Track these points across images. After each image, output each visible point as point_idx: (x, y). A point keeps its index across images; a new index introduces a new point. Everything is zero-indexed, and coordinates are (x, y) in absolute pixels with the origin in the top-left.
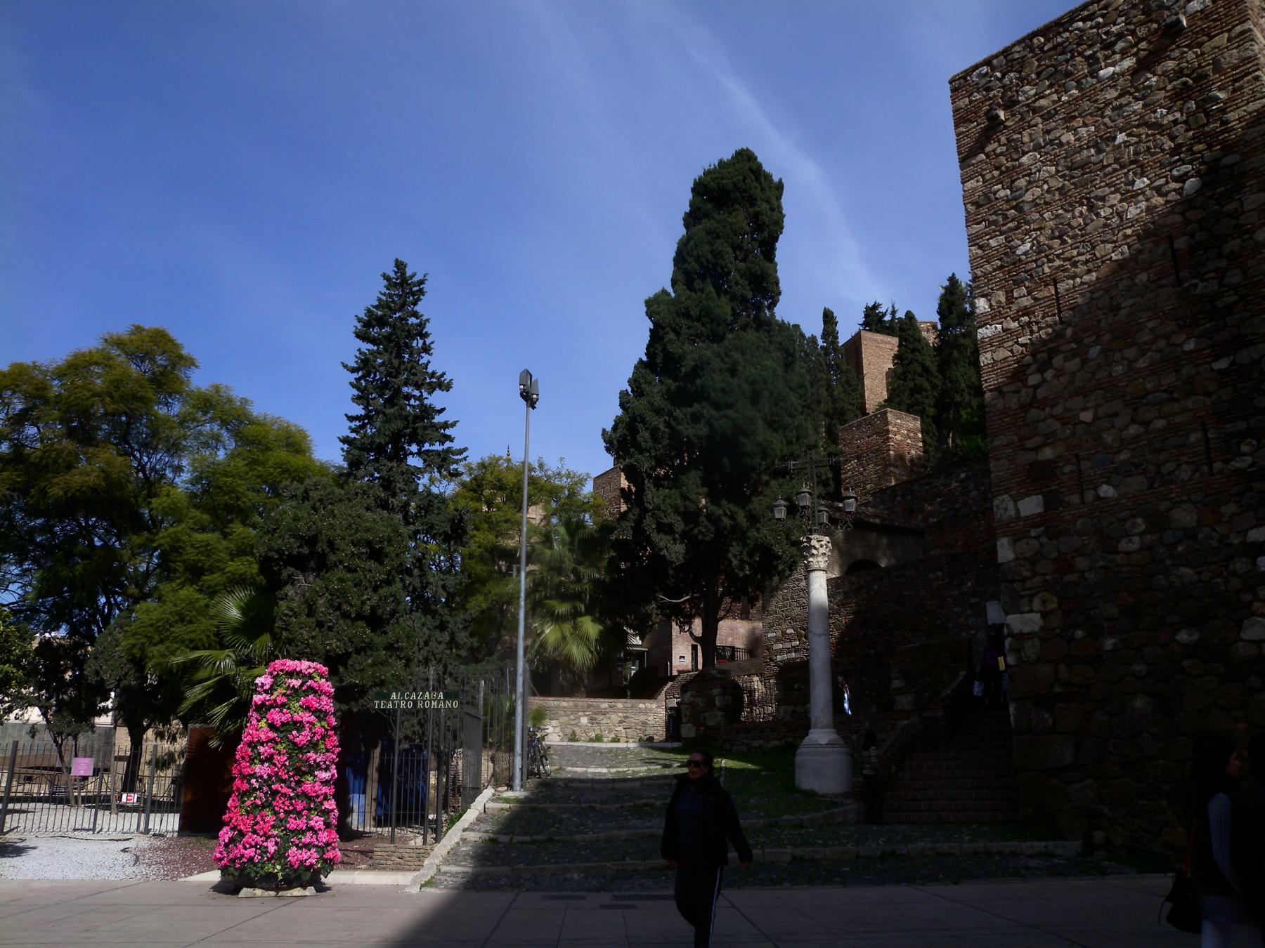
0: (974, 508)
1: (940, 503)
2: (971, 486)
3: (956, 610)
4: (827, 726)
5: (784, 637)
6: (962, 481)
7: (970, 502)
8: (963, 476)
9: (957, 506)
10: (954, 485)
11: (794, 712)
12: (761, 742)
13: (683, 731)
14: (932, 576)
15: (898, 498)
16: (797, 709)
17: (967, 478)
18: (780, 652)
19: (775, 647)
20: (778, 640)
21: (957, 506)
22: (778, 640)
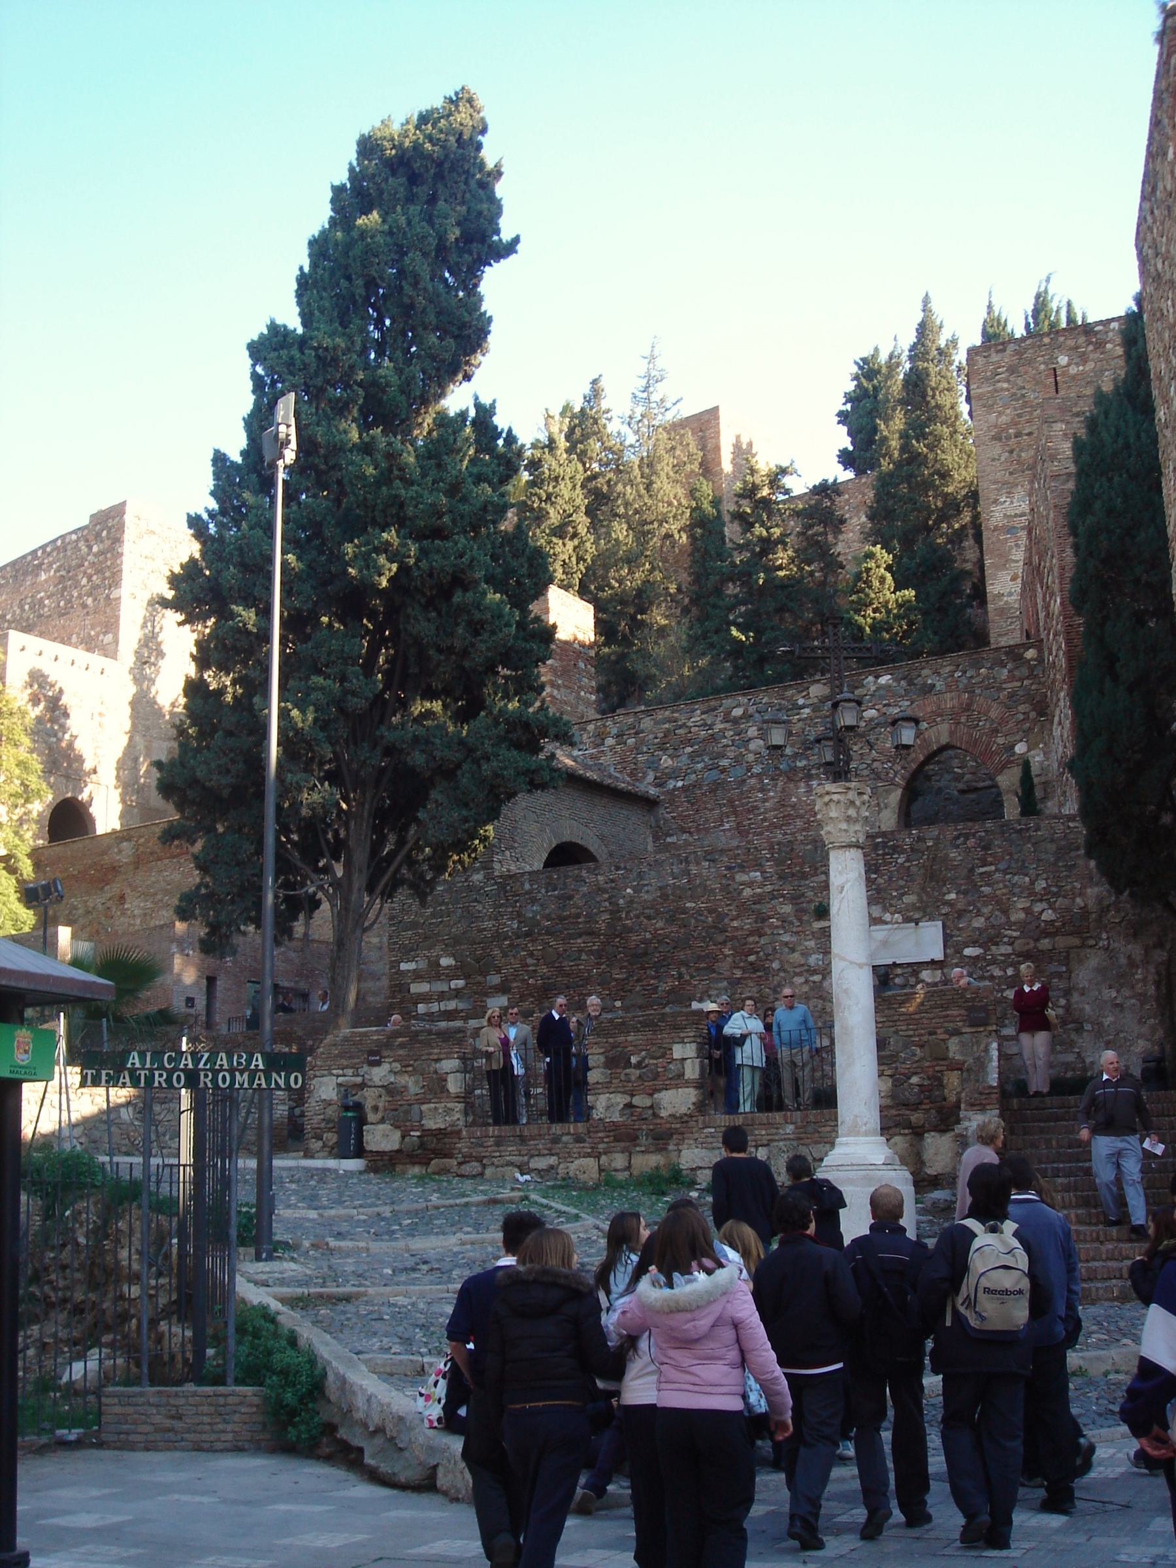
0: (757, 770)
1: (692, 756)
2: (752, 732)
3: (786, 938)
4: (873, 1134)
5: (434, 972)
6: (736, 721)
7: (751, 757)
8: (738, 712)
9: (724, 762)
10: (719, 726)
11: (629, 1106)
12: (553, 1160)
13: (367, 1137)
14: (741, 877)
15: (610, 741)
16: (637, 1101)
17: (747, 716)
18: (425, 998)
19: (418, 988)
20: (418, 976)
21: (724, 762)
22: (418, 976)
